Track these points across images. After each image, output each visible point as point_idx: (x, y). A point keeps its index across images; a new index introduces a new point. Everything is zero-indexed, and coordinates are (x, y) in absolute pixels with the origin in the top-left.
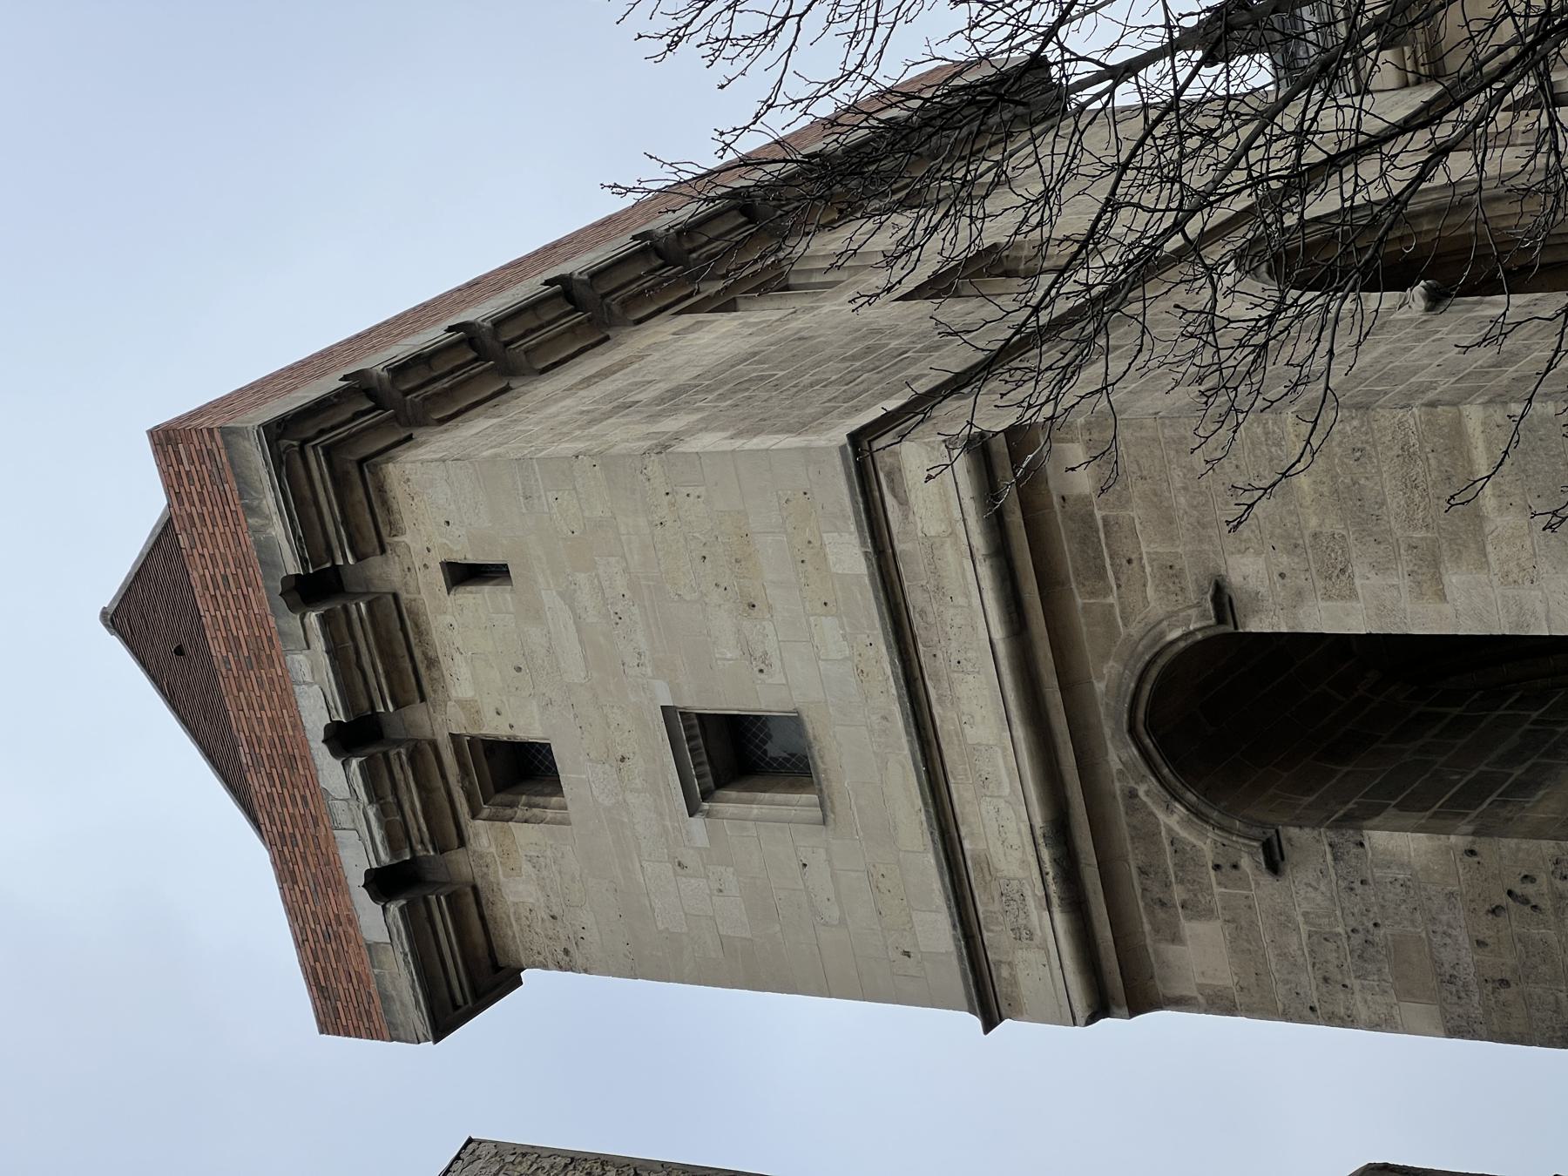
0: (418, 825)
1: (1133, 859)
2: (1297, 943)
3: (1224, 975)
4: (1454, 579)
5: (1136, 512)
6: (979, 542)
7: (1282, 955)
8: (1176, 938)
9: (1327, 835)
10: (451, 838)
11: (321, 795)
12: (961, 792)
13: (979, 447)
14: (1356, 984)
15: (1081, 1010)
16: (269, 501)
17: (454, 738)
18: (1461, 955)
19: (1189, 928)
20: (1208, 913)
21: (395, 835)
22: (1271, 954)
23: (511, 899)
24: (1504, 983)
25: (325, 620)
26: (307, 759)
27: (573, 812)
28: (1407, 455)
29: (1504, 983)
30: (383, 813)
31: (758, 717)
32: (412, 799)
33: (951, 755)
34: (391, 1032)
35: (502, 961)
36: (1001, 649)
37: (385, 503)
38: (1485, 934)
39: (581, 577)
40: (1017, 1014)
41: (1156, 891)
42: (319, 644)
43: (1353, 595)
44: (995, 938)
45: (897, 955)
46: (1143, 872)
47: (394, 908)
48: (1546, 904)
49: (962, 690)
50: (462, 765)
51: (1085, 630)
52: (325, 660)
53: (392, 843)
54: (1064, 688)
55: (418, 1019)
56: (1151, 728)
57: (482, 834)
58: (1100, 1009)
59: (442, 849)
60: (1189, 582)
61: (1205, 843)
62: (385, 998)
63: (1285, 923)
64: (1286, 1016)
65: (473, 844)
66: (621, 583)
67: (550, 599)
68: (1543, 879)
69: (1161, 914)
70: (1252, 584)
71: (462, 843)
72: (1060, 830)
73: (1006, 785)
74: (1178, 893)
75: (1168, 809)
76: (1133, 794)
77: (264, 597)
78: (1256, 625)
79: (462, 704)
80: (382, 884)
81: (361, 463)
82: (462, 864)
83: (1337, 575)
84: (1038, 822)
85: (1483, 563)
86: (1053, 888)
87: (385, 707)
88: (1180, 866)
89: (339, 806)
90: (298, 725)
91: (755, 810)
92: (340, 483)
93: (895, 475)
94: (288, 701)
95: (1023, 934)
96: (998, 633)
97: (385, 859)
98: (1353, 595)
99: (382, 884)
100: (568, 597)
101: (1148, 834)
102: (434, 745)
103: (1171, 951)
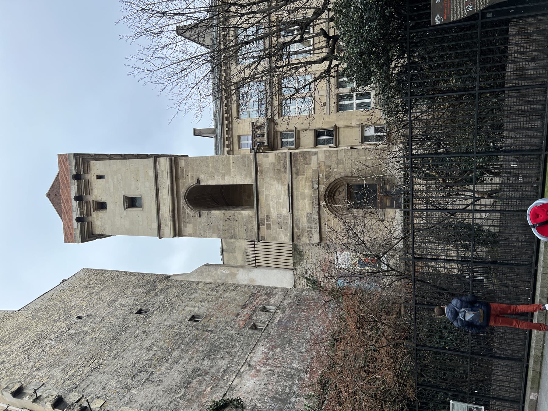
0: (85, 212)
1: (182, 216)
2: (201, 227)
4: (227, 177)
6: (169, 171)
7: (199, 228)
8: (186, 227)
9: (207, 212)
10: (89, 214)
11: (71, 206)
12: (161, 205)
14: (207, 232)
15: (172, 236)
16: (73, 164)
17: (93, 200)
18: (221, 227)
19: (188, 225)
20: (191, 223)
21: (81, 213)
22: (198, 228)
23: (96, 224)
24: (226, 230)
25: (77, 181)
26: (71, 202)
28: (223, 161)
29: (226, 230)
30: (80, 209)
31: (136, 197)
32: (85, 208)
33: (160, 200)
34: (75, 242)
35: (93, 233)
36: (169, 185)
37: (90, 167)
38: (224, 224)
39: (115, 177)
41: (184, 220)
42: (76, 184)
43: (214, 180)
44: (162, 226)
45: (149, 229)
46: (183, 218)
47: (79, 223)
48: (232, 219)
49: (163, 191)
50: (93, 205)
51: (181, 185)
52: (76, 187)
53: (81, 215)
54: (177, 192)
55: (79, 240)
56: (187, 198)
57: (94, 214)
58: (175, 236)
59: (88, 216)
60: (195, 178)
62: (75, 237)
63: (200, 224)
64: (198, 237)
65: (92, 216)
66: (120, 178)
67: (110, 180)
68: (232, 216)
69: (185, 223)
70: (202, 178)
71: (91, 216)
72: (173, 210)
73: (167, 204)
74: (187, 220)
75: (188, 209)
76: (184, 207)
77: (70, 177)
78: (202, 184)
79: (95, 195)
80: (78, 220)
81: (87, 161)
82: (90, 219)
83: (213, 177)
84: (171, 209)
85: (230, 175)
86: (171, 218)
87: (82, 173)
88: (188, 217)
89: (74, 208)
90: (70, 196)
91: (133, 210)
92: (84, 163)
93: (159, 162)
94: (70, 193)
95: (166, 225)
96: (169, 183)
97: (79, 216)
98: (214, 180)
99: (78, 220)
100: (113, 180)
101: (184, 213)
102: (90, 201)
103: (185, 229)
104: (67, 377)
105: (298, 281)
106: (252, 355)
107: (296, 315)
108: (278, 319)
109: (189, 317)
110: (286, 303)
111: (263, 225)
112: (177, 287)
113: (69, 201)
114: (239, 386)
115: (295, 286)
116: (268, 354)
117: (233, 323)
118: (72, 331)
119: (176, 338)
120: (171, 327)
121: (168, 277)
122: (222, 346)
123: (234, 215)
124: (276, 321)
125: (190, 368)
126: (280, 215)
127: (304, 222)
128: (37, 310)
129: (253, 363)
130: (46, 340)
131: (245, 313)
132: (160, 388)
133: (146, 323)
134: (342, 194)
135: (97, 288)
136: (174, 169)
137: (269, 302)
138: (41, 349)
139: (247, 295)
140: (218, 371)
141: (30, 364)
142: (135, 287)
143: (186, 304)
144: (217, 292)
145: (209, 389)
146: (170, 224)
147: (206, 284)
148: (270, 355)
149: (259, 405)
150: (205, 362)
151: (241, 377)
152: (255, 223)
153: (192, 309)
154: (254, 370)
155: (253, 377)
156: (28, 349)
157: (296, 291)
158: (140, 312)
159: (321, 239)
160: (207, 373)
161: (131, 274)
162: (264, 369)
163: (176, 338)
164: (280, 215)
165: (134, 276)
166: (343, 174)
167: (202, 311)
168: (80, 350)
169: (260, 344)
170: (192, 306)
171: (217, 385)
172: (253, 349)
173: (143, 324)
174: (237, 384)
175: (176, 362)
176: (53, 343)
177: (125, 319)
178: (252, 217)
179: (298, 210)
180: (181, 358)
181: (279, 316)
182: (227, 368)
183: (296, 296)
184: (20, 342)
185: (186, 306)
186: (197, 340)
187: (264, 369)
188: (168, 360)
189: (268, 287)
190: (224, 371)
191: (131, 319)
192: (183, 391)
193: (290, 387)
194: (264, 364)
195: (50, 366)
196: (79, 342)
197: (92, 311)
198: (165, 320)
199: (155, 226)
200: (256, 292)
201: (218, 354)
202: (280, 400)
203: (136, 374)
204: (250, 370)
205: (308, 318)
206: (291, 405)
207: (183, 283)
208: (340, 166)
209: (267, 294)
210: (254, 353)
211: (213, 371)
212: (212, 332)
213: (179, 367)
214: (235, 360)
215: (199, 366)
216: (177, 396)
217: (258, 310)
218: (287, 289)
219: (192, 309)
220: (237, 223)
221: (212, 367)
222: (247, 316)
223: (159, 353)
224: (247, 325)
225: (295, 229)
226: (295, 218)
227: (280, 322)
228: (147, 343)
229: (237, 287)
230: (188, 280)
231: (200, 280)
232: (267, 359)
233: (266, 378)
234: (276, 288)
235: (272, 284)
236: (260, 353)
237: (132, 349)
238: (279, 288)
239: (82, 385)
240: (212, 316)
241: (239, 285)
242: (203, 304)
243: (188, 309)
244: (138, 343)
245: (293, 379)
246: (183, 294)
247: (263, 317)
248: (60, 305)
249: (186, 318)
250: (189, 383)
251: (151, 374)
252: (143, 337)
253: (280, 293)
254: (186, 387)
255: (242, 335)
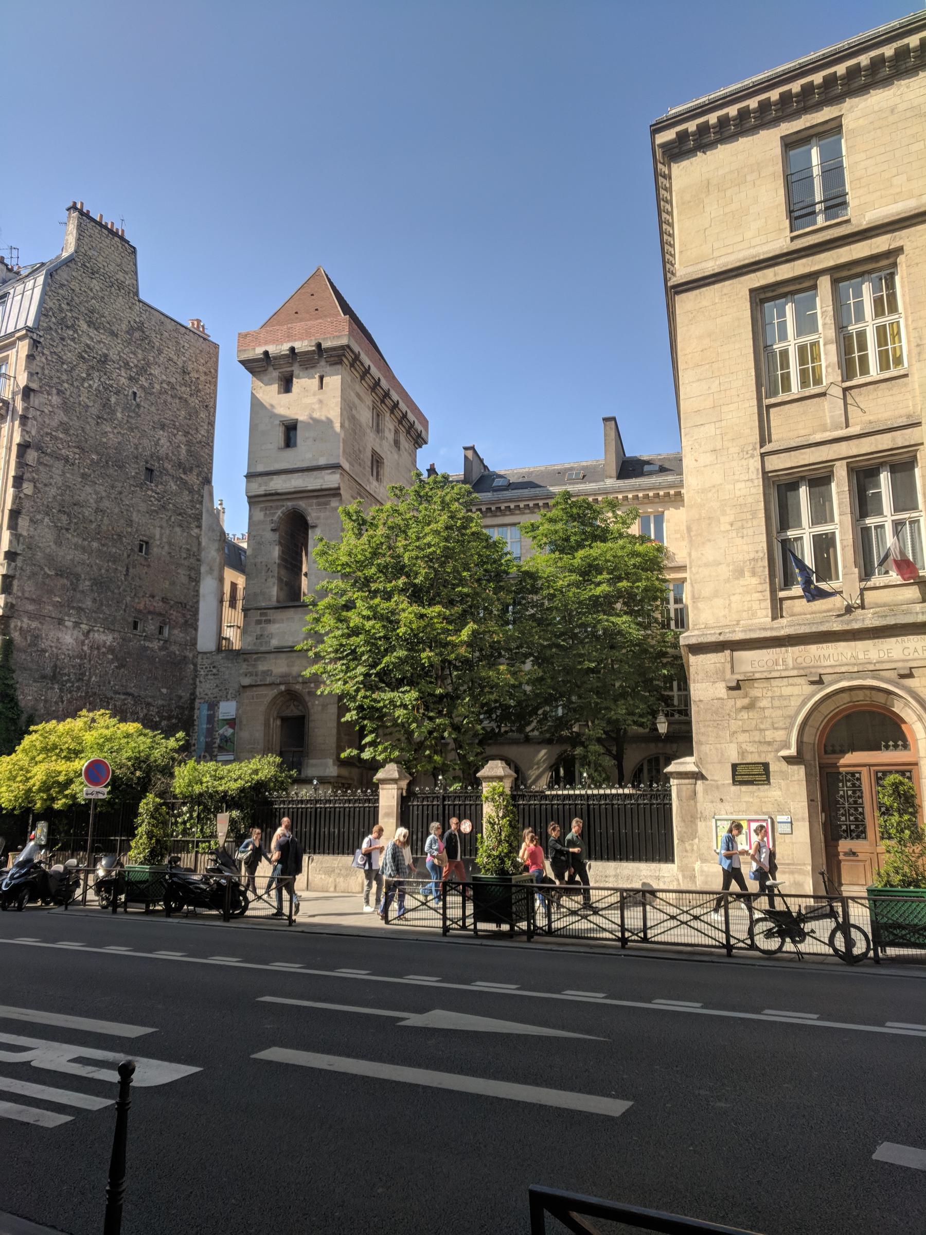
3: (255, 518)
5: (328, 513)
6: (324, 487)
12: (283, 477)
13: (339, 488)
15: (250, 494)
18: (259, 560)
19: (262, 514)
21: (275, 358)
26: (289, 341)
27: (280, 396)
33: (290, 476)
40: (248, 482)
51: (310, 501)
54: (301, 498)
57: (276, 374)
58: (248, 497)
61: (275, 518)
72: (277, 494)
78: (310, 531)
82: (271, 369)
90: (295, 340)
95: (260, 485)
96: (309, 488)
101: (277, 508)
104: (54, 433)
105: (205, 656)
106: (101, 630)
107: (157, 665)
108: (151, 646)
109: (145, 538)
110: (175, 648)
111: (261, 615)
112: (191, 501)
113: (289, 337)
114: (64, 629)
115: (199, 653)
116: (104, 646)
117: (141, 594)
118: (113, 400)
119: (115, 537)
120: (130, 523)
121: (208, 481)
122: (109, 594)
123: (273, 577)
124: (147, 644)
125: (79, 569)
126: (271, 636)
127: (262, 667)
128: (141, 327)
129: (91, 635)
130: (97, 374)
131: (155, 604)
132: (53, 547)
133: (132, 489)
134: (293, 711)
135: (183, 388)
136: (327, 493)
137: (174, 628)
138: (84, 375)
139: (182, 597)
140: (80, 601)
141: (64, 377)
142: (189, 444)
143: (165, 525)
144: (185, 559)
145: (58, 599)
146: (261, 491)
147: (198, 537)
148: (104, 650)
149: (47, 654)
150: (87, 583)
151: (74, 628)
152: (263, 604)
153: (158, 537)
154: (83, 638)
155: (76, 640)
156: (83, 358)
157: (194, 656)
158: (150, 471)
159: (244, 687)
160: (74, 590)
161: (212, 424)
162: (85, 648)
163: (115, 537)
164: (271, 636)
165: (208, 431)
166: (312, 711)
167: (155, 550)
168: (88, 427)
169: (116, 635)
170: (161, 535)
171: (61, 606)
172: (108, 629)
173: (131, 485)
174: (66, 627)
175: (84, 549)
176: (96, 385)
177: (137, 458)
178: (270, 600)
179: (276, 658)
180: (90, 554)
181: (155, 645)
182: (82, 609)
183: (185, 657)
184: (91, 338)
185: (161, 527)
186: (114, 562)
187: (85, 648)
188: (84, 539)
189: (197, 620)
190: (80, 607)
191: (137, 466)
192: (53, 573)
193: (69, 681)
194: (91, 647)
195: (66, 407)
196: (99, 418)
197: (146, 406)
198: (139, 511)
199: (260, 468)
200: (188, 607)
201: (99, 593)
202: (54, 672)
203: (65, 512)
204: (83, 634)
205: (156, 678)
206: (50, 685)
207: (198, 506)
208: (320, 708)
209: (186, 622)
210: (104, 632)
211: (78, 595)
212: (127, 575)
213: (80, 556)
214: (94, 615)
215: (83, 576)
216: (46, 569)
217: (161, 619)
218: (196, 644)
219: (158, 537)
220: (263, 581)
221: (83, 592)
222: (152, 609)
223: (93, 526)
224: (140, 611)
225: (255, 656)
226: (266, 655)
227: (146, 648)
228: (106, 504)
229: (195, 580)
230: (204, 511)
231: (203, 528)
232: (98, 648)
233: (75, 654)
234: (196, 629)
235: (201, 625)
236: (105, 638)
237: (95, 491)
238: (196, 634)
239: (47, 457)
240: (149, 566)
241: (199, 582)
242: (166, 548)
243: (157, 532)
244: (104, 494)
245: (78, 681)
246: (180, 514)
247: (151, 627)
248: (152, 354)
249: (144, 535)
250: (61, 576)
251: (67, 530)
252: (113, 496)
253: (188, 638)
254: (57, 575)
255: (125, 610)
